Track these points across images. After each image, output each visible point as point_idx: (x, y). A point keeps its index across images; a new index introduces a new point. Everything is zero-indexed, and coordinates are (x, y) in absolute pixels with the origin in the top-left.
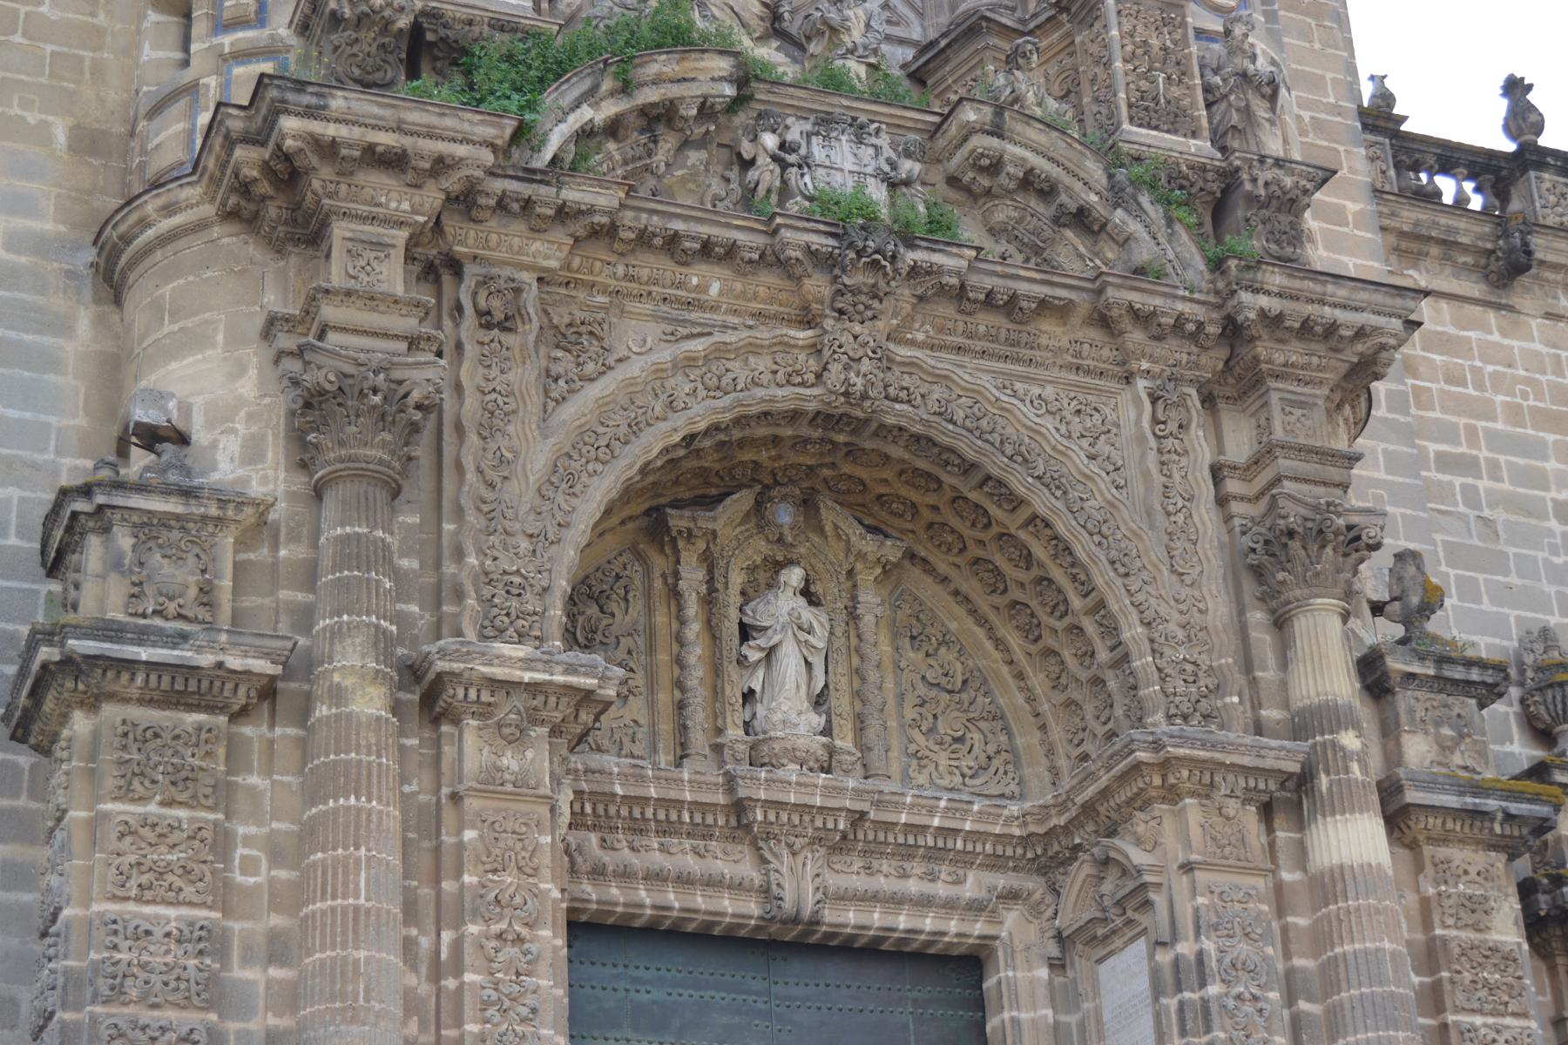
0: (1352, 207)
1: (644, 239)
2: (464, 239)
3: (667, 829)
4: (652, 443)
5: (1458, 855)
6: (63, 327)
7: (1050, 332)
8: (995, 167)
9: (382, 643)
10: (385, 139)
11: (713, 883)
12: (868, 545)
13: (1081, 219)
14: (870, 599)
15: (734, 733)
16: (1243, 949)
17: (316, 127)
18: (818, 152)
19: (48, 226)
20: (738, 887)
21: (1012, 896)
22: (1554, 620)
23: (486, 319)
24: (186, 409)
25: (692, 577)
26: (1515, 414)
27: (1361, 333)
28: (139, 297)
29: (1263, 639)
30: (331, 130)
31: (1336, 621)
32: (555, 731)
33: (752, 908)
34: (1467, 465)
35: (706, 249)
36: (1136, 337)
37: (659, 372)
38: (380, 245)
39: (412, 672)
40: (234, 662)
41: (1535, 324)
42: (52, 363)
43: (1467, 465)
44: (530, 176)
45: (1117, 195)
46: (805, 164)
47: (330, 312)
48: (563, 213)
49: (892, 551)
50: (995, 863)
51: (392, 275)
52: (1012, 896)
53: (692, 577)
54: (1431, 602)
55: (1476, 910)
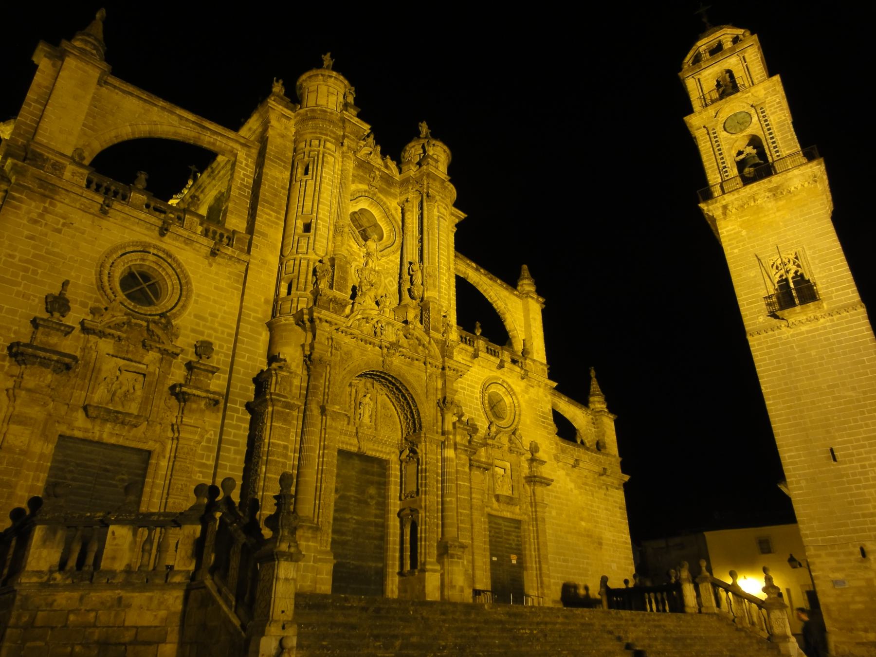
3: (346, 435)
10: (328, 319)
13: (424, 346)
17: (319, 315)
19: (260, 316)
20: (355, 446)
22: (473, 416)
29: (440, 418)
30: (321, 316)
36: (429, 366)
40: (296, 403)
45: (429, 343)
46: (385, 330)
50: (392, 446)
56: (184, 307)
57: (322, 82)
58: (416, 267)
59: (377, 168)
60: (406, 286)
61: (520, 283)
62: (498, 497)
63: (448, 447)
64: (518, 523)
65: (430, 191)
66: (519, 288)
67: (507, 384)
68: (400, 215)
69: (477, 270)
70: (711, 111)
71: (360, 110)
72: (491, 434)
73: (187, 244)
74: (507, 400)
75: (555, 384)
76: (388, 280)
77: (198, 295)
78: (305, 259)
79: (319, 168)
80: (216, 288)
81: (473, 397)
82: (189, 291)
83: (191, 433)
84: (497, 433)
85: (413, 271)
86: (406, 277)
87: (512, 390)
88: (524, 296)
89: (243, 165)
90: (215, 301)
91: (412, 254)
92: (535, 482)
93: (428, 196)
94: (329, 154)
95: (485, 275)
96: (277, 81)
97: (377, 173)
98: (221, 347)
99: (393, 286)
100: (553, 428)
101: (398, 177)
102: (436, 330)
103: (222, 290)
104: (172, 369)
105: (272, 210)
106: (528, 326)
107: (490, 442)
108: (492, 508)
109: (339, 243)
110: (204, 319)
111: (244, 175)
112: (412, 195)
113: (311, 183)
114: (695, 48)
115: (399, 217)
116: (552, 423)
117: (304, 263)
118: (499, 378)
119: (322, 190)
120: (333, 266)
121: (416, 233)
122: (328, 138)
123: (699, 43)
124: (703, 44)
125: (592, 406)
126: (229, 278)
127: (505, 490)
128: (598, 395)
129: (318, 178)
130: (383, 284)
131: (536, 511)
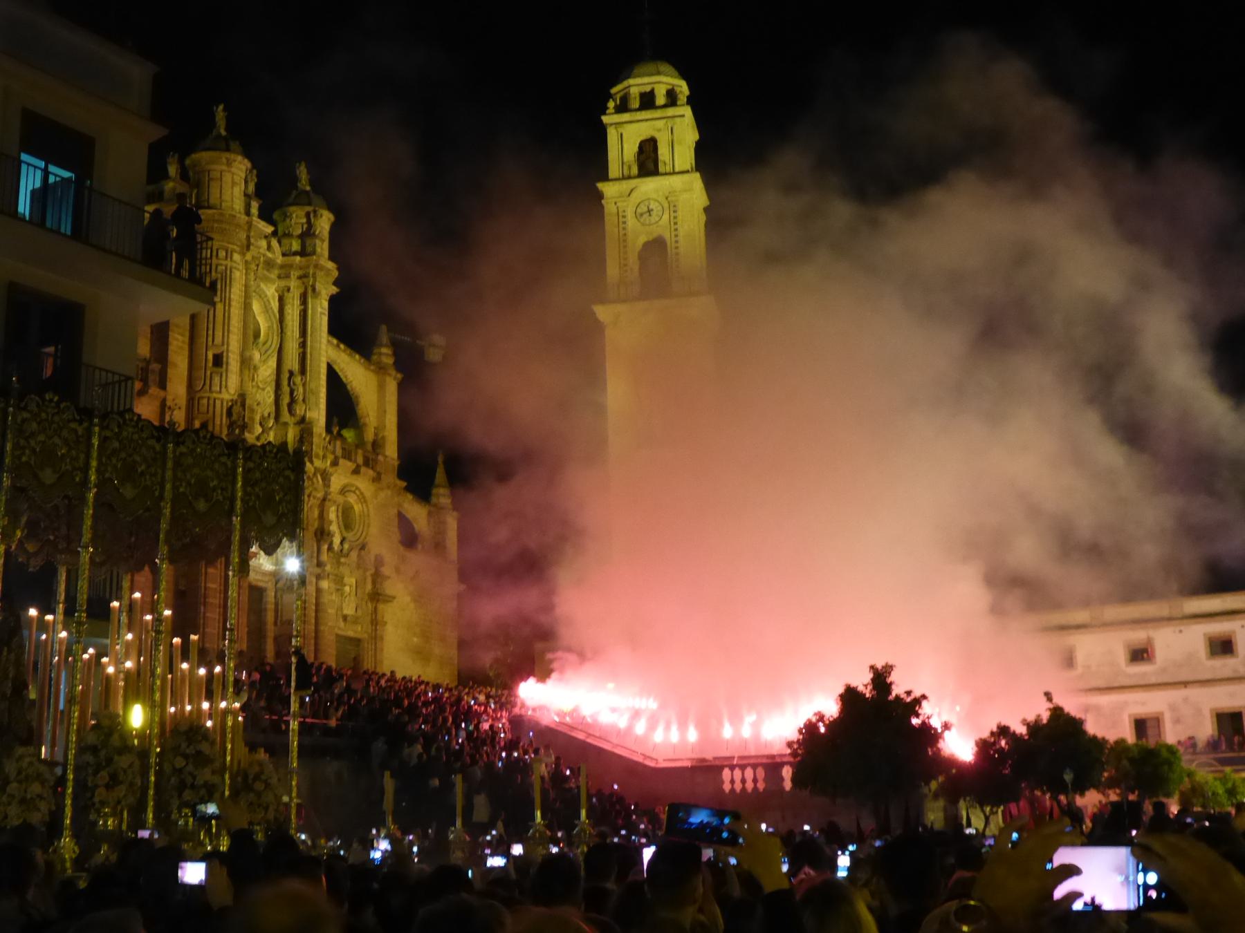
57: (224, 167)
58: (298, 379)
60: (286, 400)
61: (376, 351)
62: (345, 618)
63: (323, 578)
64: (357, 642)
65: (318, 286)
66: (375, 358)
67: (360, 490)
68: (277, 304)
69: (338, 346)
70: (626, 185)
71: (261, 202)
72: (345, 551)
74: (357, 508)
75: (405, 484)
78: (219, 399)
79: (228, 288)
84: (351, 550)
85: (294, 384)
86: (286, 389)
87: (364, 497)
88: (380, 369)
91: (292, 362)
92: (378, 601)
93: (314, 290)
95: (344, 351)
96: (173, 156)
99: (270, 397)
100: (396, 536)
101: (280, 260)
102: (317, 456)
106: (382, 412)
107: (343, 560)
108: (339, 628)
109: (246, 378)
112: (294, 283)
114: (625, 83)
115: (275, 305)
116: (396, 530)
117: (218, 403)
118: (352, 485)
119: (232, 315)
120: (243, 405)
121: (297, 334)
122: (235, 247)
123: (631, 81)
124: (636, 85)
125: (434, 500)
127: (349, 610)
128: (443, 487)
129: (227, 301)
131: (376, 630)
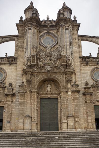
0: (78, 62)
1: (40, 72)
2: (33, 74)
4: (41, 80)
5: (75, 93)
6: (21, 78)
7: (58, 73)
8: (55, 66)
9: (29, 90)
11: (46, 96)
12: (52, 82)
13: (59, 68)
14: (53, 84)
15: (47, 90)
16: (64, 98)
18: (48, 67)
20: (47, 96)
21: (58, 96)
23: (34, 76)
24: (24, 81)
25: (45, 84)
26: (87, 71)
27: (71, 71)
28: (23, 77)
31: (70, 84)
32: (36, 92)
33: (47, 97)
34: (84, 73)
35: (42, 72)
36: (61, 73)
37: (41, 77)
38: (29, 75)
39: (30, 91)
41: (89, 66)
42: (21, 79)
43: (84, 73)
44: (35, 71)
47: (27, 78)
48: (36, 72)
49: (53, 82)
50: (58, 94)
51: (30, 76)
52: (58, 96)
53: (45, 84)
54: (76, 82)
55: (76, 95)
56: (6, 78)
59: (48, 25)
63: (69, 92)
73: (5, 64)
76: (55, 53)
77: (8, 74)
80: (12, 71)
81: (87, 75)
82: (7, 74)
83: (9, 102)
84: (95, 83)
89: (17, 41)
90: (12, 74)
94: (29, 30)
97: (48, 26)
98: (14, 83)
103: (13, 71)
104: (5, 90)
105: (21, 49)
110: (10, 78)
111: (17, 43)
113: (26, 39)
126: (14, 68)
130: (53, 55)
